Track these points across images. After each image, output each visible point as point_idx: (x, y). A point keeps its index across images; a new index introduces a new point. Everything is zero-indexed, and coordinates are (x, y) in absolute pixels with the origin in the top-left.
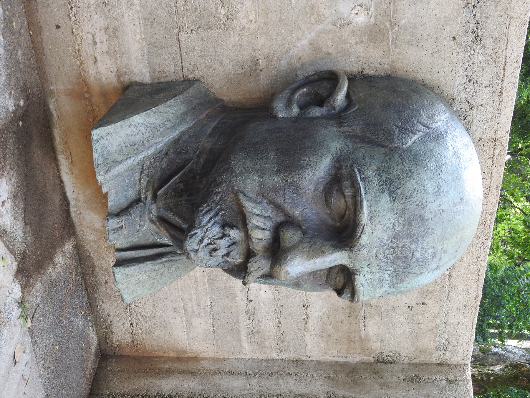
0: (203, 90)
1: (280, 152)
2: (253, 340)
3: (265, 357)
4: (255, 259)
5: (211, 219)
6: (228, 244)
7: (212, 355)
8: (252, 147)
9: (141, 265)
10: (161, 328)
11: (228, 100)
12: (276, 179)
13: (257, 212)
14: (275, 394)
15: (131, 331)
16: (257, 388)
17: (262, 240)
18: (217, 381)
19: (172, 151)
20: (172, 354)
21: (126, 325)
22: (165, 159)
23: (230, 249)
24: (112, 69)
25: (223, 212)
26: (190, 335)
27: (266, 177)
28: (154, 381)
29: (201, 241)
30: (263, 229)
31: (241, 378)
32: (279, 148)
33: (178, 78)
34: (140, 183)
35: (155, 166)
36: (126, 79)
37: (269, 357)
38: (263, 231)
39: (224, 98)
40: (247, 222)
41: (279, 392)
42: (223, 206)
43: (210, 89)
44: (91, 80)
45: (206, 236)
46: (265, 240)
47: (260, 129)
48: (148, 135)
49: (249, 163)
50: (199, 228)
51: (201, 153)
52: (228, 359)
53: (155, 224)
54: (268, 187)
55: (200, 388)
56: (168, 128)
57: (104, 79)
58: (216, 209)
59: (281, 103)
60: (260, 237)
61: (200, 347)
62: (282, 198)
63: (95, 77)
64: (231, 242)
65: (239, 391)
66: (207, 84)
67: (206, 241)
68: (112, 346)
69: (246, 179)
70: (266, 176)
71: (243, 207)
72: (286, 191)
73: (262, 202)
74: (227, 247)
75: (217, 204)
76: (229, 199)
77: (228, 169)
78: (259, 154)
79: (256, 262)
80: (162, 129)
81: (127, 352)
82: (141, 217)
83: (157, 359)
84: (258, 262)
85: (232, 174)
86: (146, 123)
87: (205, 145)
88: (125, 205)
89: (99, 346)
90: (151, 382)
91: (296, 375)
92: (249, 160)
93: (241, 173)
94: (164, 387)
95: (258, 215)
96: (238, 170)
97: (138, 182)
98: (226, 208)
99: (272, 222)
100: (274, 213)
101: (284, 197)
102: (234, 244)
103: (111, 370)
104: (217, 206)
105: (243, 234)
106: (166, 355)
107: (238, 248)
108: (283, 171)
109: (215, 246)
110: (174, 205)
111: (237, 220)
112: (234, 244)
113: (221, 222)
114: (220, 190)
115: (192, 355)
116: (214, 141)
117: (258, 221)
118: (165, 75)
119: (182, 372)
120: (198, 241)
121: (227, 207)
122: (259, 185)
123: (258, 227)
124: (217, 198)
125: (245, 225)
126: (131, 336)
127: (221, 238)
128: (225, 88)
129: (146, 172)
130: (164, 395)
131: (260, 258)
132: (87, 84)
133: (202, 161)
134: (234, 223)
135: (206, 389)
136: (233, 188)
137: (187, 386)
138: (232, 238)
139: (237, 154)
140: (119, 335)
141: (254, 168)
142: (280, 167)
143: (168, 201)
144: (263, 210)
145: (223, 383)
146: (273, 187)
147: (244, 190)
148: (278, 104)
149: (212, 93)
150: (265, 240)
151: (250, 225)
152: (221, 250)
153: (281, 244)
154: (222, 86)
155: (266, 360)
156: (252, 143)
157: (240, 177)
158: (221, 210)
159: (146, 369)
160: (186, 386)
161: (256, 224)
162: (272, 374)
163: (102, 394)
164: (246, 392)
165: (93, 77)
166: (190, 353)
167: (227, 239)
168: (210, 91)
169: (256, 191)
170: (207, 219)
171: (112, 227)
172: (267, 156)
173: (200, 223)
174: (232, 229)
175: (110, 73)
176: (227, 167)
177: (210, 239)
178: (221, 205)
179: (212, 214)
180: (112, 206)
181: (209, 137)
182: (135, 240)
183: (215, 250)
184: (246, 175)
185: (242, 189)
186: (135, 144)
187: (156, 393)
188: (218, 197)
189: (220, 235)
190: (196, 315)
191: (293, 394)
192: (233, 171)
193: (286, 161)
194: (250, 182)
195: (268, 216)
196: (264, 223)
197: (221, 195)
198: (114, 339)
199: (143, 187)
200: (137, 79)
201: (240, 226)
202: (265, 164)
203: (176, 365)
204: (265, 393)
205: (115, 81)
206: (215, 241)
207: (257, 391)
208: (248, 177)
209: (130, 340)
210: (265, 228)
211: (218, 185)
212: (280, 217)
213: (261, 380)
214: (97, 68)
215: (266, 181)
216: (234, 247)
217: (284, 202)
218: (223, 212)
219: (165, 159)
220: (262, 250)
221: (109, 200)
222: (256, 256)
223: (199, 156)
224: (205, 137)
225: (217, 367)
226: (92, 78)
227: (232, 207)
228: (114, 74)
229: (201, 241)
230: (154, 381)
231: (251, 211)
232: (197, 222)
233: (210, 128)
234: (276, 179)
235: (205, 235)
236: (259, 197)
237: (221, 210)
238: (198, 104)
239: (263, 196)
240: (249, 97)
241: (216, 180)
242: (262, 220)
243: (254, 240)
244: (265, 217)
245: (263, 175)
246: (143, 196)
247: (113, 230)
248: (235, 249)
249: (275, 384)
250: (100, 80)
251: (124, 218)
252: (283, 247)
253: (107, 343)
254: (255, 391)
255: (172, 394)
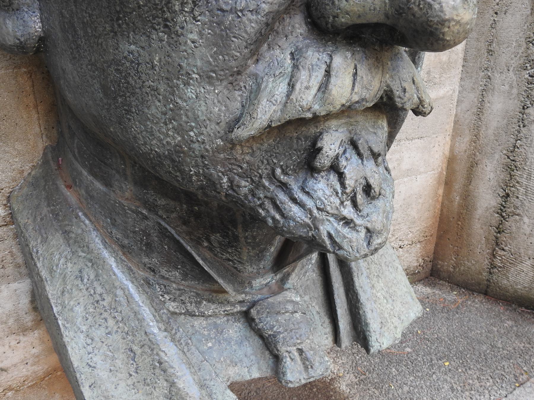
0: (26, 189)
1: (119, 26)
2: (437, 80)
3: (460, 62)
4: (397, 92)
5: (294, 200)
6: (355, 158)
7: (448, 139)
8: (115, 98)
9: (363, 297)
10: (409, 210)
11: (44, 138)
12: (191, 36)
13: (282, 88)
14: (525, 46)
15: (409, 246)
16: (511, 73)
17: (355, 74)
18: (490, 132)
19: (146, 260)
20: (441, 192)
21: (401, 253)
22: (163, 272)
23: (366, 153)
24: (13, 343)
25: (278, 171)
26: (422, 170)
27: (188, 64)
28: (478, 217)
29: (348, 222)
30: (328, 73)
31: (490, 97)
32: (108, 29)
33: (11, 234)
34: (215, 315)
35: (178, 292)
36: (28, 319)
37: (461, 55)
38: (333, 73)
39: (41, 146)
40: (309, 115)
41: (523, 39)
42: (264, 171)
43: (26, 174)
44: (40, 369)
45: (336, 212)
46: (356, 68)
47: (73, 78)
48: (111, 322)
49: (153, 110)
50: (317, 228)
51: (145, 204)
52: (456, 115)
53: (289, 275)
54: (215, 60)
55: (497, 156)
56: (97, 276)
57: (34, 351)
58: (272, 188)
59: (5, 24)
60: (348, 80)
61: (437, 156)
62: (244, 19)
63: (32, 366)
64: (351, 153)
65: (511, 102)
66: (14, 180)
67: (348, 211)
68: (422, 266)
69: (196, 119)
70: (184, 65)
71: (269, 126)
72: (224, 7)
73: (255, 76)
74: (362, 160)
75: (259, 185)
76: (248, 158)
77: (173, 161)
78: (128, 83)
79: (405, 91)
80: (99, 290)
81: (431, 247)
82: (278, 313)
83: (445, 211)
84: (405, 85)
85: (183, 152)
86: (84, 328)
87: (127, 194)
88: (257, 341)
89: (421, 280)
90: (479, 219)
91: (496, 13)
92: (146, 110)
93: (180, 130)
94: (490, 204)
95: (291, 86)
96: (174, 138)
97: (212, 320)
98: (268, 164)
99: (308, 46)
100: (282, 42)
101: (241, 11)
102: (354, 144)
103: (454, 268)
104: (264, 187)
105: (333, 123)
106: (440, 199)
107: (363, 133)
108: (168, 15)
109: (359, 190)
110: (253, 248)
111: (298, 138)
112: (354, 144)
113: (302, 175)
114: (225, 180)
115: (445, 165)
116: (117, 176)
117: (307, 88)
118: (9, 257)
119: (469, 178)
120: (345, 231)
121: (265, 162)
122: (211, 84)
123: (324, 87)
124: (245, 186)
125: (316, 119)
126: (414, 245)
127: (341, 176)
128: (18, 146)
129: (192, 308)
130: (502, 205)
131: (398, 81)
132: (48, 374)
133: (162, 202)
134: (305, 144)
135: (500, 148)
136: (218, 150)
137: (492, 174)
138: (342, 150)
139: (135, 137)
140: (411, 260)
141: (165, 97)
142: (159, 24)
143: (245, 258)
144: (277, 73)
145: (494, 124)
146: (215, 45)
147: (223, 124)
148: (8, 34)
149: (32, 170)
150: (356, 68)
151: (316, 107)
152: (369, 174)
153: (375, 20)
154: (15, 153)
155: (465, 60)
156: (105, 101)
157: (192, 134)
158: (272, 176)
159: (459, 224)
160: (492, 176)
161: (314, 91)
162: (490, 52)
163: (488, 280)
164: (515, 91)
165: (33, 367)
166: (442, 168)
167: (343, 162)
168: (30, 174)
169: (226, 92)
170: (295, 210)
171: (300, 373)
172: (132, 62)
173: (306, 225)
174: (320, 149)
175: (22, 344)
176: (167, 162)
177: (342, 203)
178: (261, 177)
179: (282, 196)
180: (259, 369)
181: (111, 186)
182: (317, 308)
183: (368, 189)
184: (184, 118)
185: (221, 129)
186: (131, 350)
187: (497, 215)
188: (243, 183)
189: (333, 178)
190: (399, 164)
191: (530, 18)
192: (178, 150)
193: (139, 7)
194: (203, 108)
195: (293, 59)
196: (311, 70)
197: (237, 178)
198: (416, 264)
199: (221, 310)
200: (25, 301)
201: (313, 130)
202: (153, 67)
203: (458, 186)
204: (522, 61)
205: (36, 333)
206: (348, 190)
207: (515, 74)
208: (190, 114)
209: (418, 246)
210: (324, 67)
211: (213, 184)
212: (293, 27)
213: (498, 68)
214: (15, 365)
215: (199, 63)
216: (361, 144)
217: (256, 11)
218: (278, 171)
219: (163, 272)
220: (379, 76)
221: (248, 378)
222: (391, 91)
223: (153, 208)
224: (112, 195)
225: (467, 132)
226: (36, 368)
227: (266, 151)
228: (21, 338)
229: (348, 222)
230: (478, 217)
231: (280, 107)
232: (302, 232)
233: (93, 183)
234: (191, 36)
235: (333, 215)
236: (242, 84)
237: (272, 176)
238: (48, 205)
239: (239, 73)
240: (32, 96)
241: (202, 188)
242: (303, 75)
243: (356, 98)
244: (296, 67)
245: (183, 72)
246: (238, 308)
247: (306, 368)
248: (367, 142)
249: (508, 47)
250: (37, 357)
251: (283, 349)
252: (387, 16)
253: (419, 272)
254: (514, 78)
255: (501, 195)
